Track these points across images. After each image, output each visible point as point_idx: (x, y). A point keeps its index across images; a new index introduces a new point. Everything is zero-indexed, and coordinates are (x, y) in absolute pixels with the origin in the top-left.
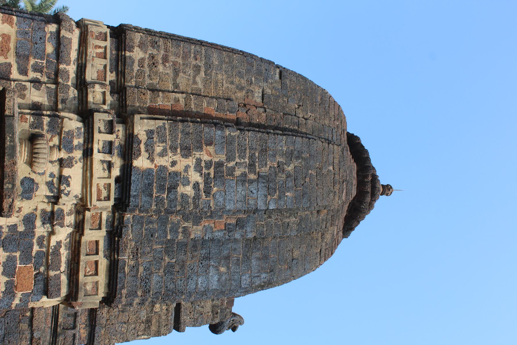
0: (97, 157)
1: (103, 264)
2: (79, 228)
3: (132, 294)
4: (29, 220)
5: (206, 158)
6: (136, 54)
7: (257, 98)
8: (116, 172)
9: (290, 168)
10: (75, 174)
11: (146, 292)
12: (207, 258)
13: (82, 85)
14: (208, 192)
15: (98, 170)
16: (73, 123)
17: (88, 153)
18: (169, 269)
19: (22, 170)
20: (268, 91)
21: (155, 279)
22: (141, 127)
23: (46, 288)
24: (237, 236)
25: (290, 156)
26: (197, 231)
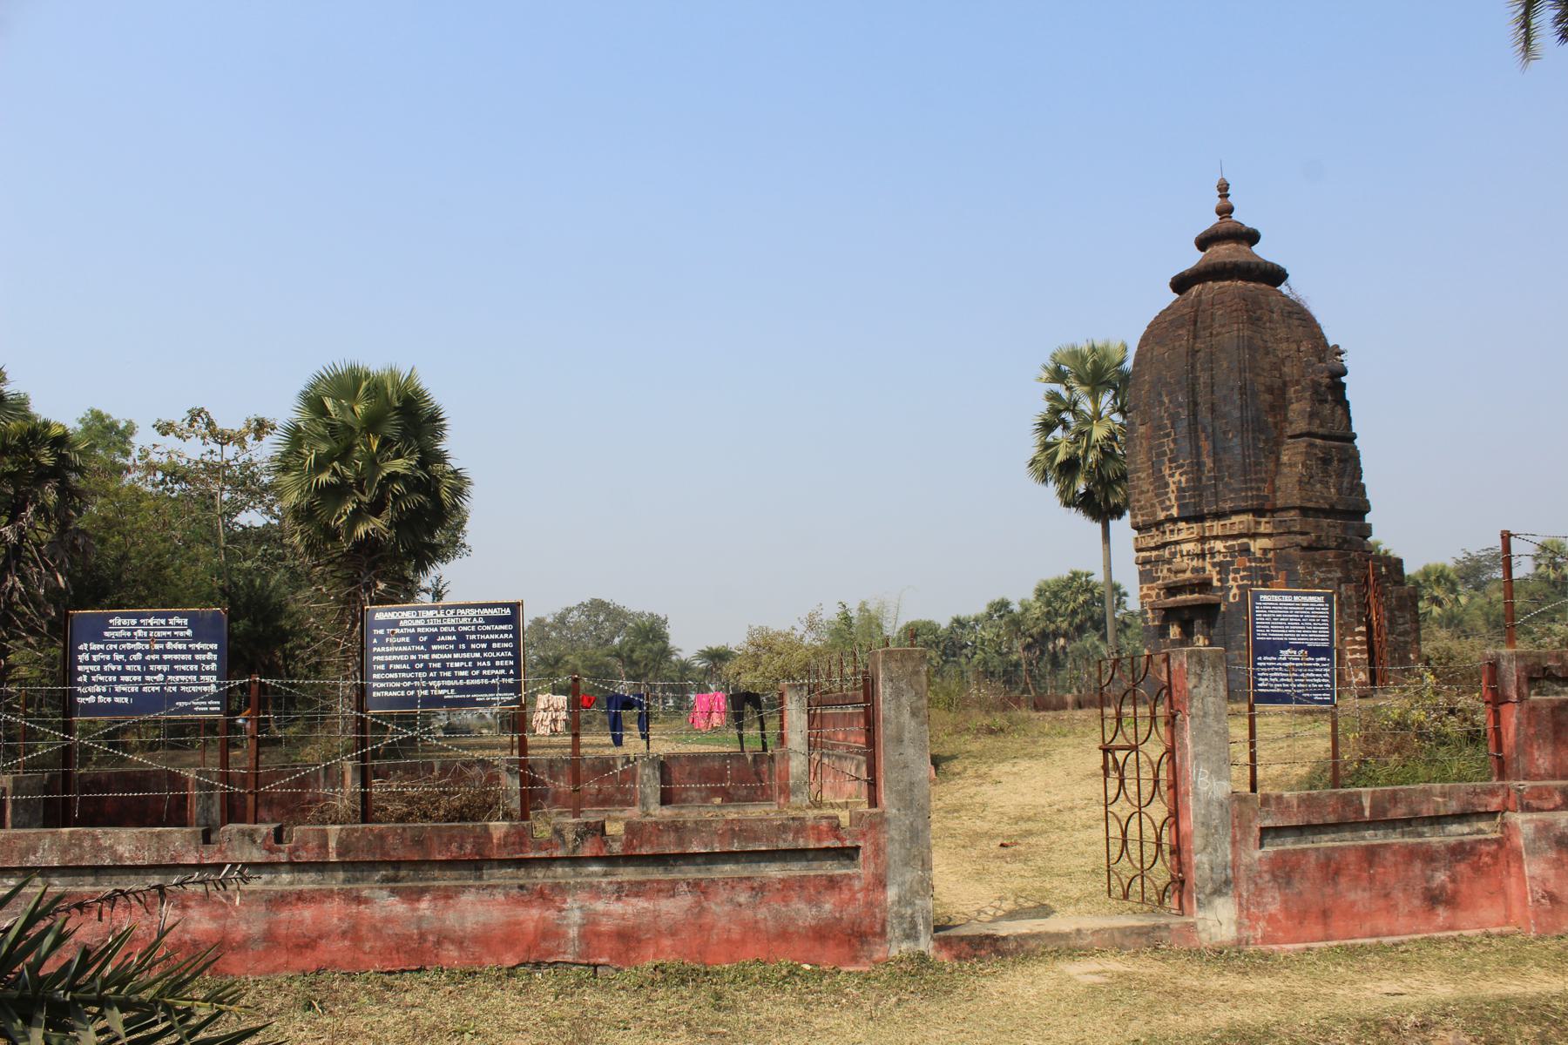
0: (1175, 538)
1: (1235, 519)
2: (1216, 538)
3: (1246, 499)
4: (1214, 565)
5: (1167, 472)
6: (1139, 519)
7: (1142, 429)
8: (1182, 525)
9: (1166, 400)
10: (1186, 547)
11: (1242, 490)
12: (1224, 449)
13: (1157, 548)
14: (1182, 466)
15: (1183, 536)
16: (1166, 553)
17: (1177, 543)
18: (1230, 476)
19: (1188, 575)
20: (1138, 421)
21: (1236, 486)
22: (1162, 515)
23: (1245, 550)
24: (1210, 430)
25: (1161, 403)
26: (1209, 463)
